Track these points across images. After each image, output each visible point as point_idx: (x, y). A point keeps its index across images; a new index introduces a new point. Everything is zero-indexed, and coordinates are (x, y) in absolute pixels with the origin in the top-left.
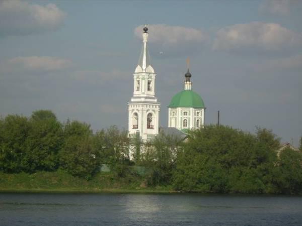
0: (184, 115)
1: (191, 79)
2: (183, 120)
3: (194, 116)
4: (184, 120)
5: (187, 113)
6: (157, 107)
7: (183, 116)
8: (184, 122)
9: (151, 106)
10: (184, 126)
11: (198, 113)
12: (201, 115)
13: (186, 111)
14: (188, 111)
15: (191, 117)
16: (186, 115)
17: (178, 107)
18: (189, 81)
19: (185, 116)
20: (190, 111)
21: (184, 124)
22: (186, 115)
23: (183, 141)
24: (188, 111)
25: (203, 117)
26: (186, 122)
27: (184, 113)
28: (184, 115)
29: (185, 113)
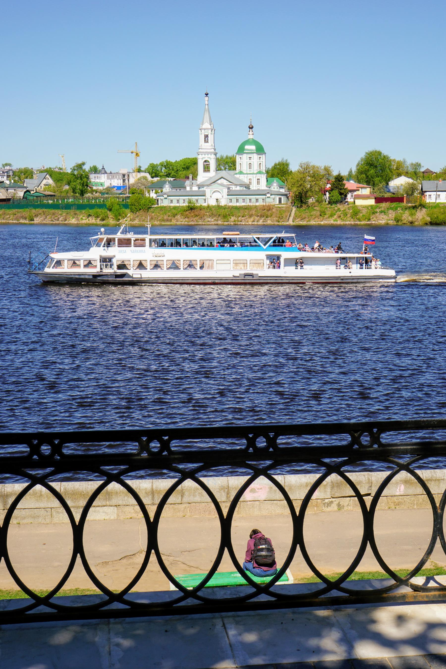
20: (253, 156)
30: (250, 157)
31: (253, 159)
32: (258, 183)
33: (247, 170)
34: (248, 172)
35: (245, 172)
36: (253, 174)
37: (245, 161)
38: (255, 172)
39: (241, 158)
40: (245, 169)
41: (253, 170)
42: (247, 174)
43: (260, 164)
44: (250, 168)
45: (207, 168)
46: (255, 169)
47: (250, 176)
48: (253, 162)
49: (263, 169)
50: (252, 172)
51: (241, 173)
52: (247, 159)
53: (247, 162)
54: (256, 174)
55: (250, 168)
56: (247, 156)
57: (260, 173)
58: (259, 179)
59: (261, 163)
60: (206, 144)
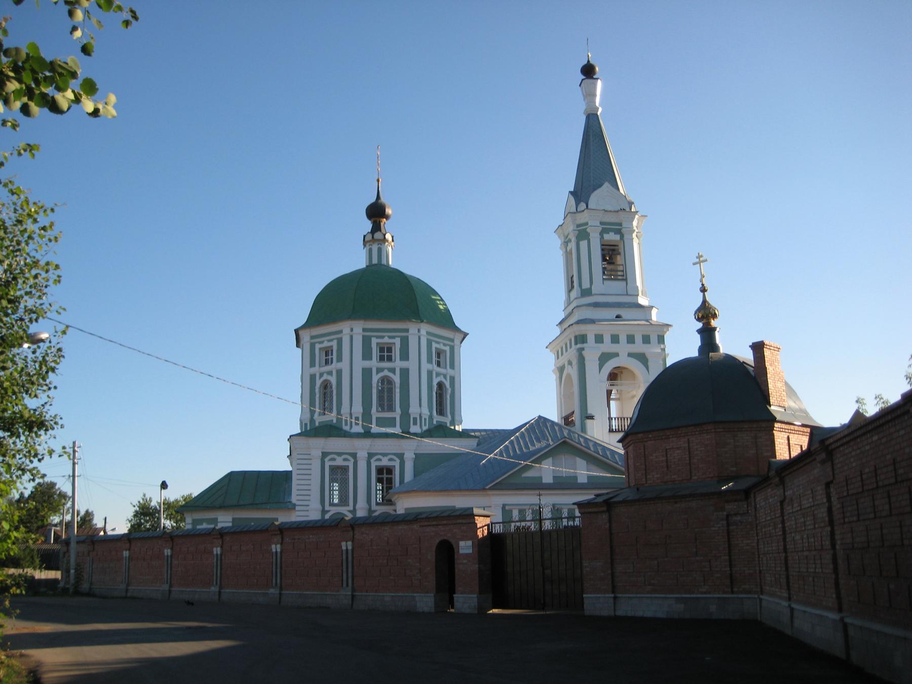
0: (382, 359)
2: (319, 382)
7: (374, 363)
13: (326, 344)
16: (390, 359)
20: (405, 342)
22: (390, 359)
23: (406, 481)
24: (397, 341)
26: (391, 391)
28: (382, 359)
29: (386, 353)
30: (386, 340)
31: (405, 356)
34: (375, 429)
35: (358, 429)
36: (406, 433)
37: (360, 364)
38: (414, 429)
39: (328, 352)
40: (358, 409)
41: (405, 414)
42: (367, 434)
43: (440, 385)
44: (386, 403)
46: (414, 410)
48: (405, 373)
50: (397, 430)
52: (367, 355)
53: (367, 373)
54: (423, 435)
55: (386, 403)
56: (366, 342)
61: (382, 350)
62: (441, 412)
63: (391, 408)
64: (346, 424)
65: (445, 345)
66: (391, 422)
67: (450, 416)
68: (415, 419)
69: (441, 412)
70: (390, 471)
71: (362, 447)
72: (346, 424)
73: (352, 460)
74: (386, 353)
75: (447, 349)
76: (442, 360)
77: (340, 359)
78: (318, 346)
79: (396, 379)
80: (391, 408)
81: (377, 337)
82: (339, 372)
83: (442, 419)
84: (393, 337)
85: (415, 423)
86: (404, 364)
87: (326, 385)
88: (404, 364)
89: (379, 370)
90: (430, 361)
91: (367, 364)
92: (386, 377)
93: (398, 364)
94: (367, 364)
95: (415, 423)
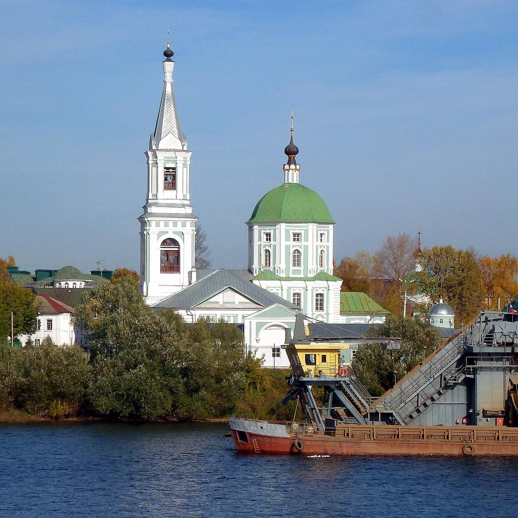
0: (294, 240)
1: (297, 157)
3: (277, 243)
4: (294, 252)
5: (298, 235)
6: (188, 224)
7: (292, 243)
8: (294, 256)
9: (171, 224)
10: (294, 265)
11: (321, 235)
12: (328, 241)
13: (268, 231)
14: (303, 232)
15: (309, 244)
17: (279, 222)
18: (295, 164)
19: (296, 243)
20: (307, 232)
21: (294, 260)
22: (298, 240)
25: (331, 244)
26: (298, 256)
27: (294, 235)
28: (294, 240)
29: (297, 237)
31: (307, 240)
32: (320, 305)
33: (288, 268)
34: (291, 276)
35: (283, 275)
38: (310, 275)
39: (268, 235)
40: (283, 266)
42: (288, 279)
45: (171, 263)
46: (310, 267)
47: (298, 286)
48: (306, 247)
49: (329, 268)
50: (302, 276)
51: (272, 276)
52: (287, 239)
53: (287, 247)
54: (314, 279)
56: (287, 231)
57: (321, 276)
58: (322, 295)
59: (325, 250)
60: (171, 194)
61: (294, 235)
62: (321, 265)
63: (299, 265)
64: (277, 273)
65: (324, 230)
66: (299, 272)
67: (326, 267)
68: (310, 270)
69: (321, 265)
70: (299, 295)
71: (286, 284)
72: (277, 273)
73: (281, 290)
74: (297, 237)
75: (326, 232)
76: (323, 238)
77: (275, 240)
78: (262, 232)
79: (302, 251)
80: (299, 265)
81: (293, 230)
82: (275, 246)
83: (322, 269)
84: (301, 230)
85: (310, 273)
86: (306, 243)
87: (267, 251)
88: (306, 243)
89: (293, 246)
90: (317, 241)
91: (288, 243)
92: (297, 250)
93: (303, 243)
94: (288, 243)
95: (310, 273)
